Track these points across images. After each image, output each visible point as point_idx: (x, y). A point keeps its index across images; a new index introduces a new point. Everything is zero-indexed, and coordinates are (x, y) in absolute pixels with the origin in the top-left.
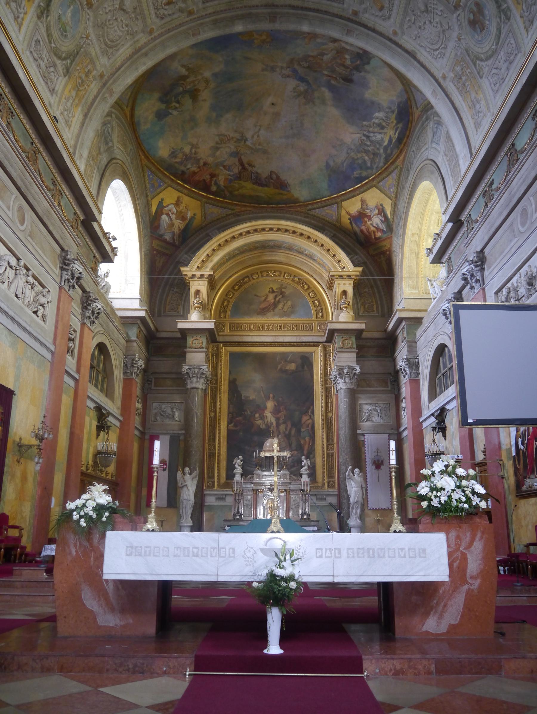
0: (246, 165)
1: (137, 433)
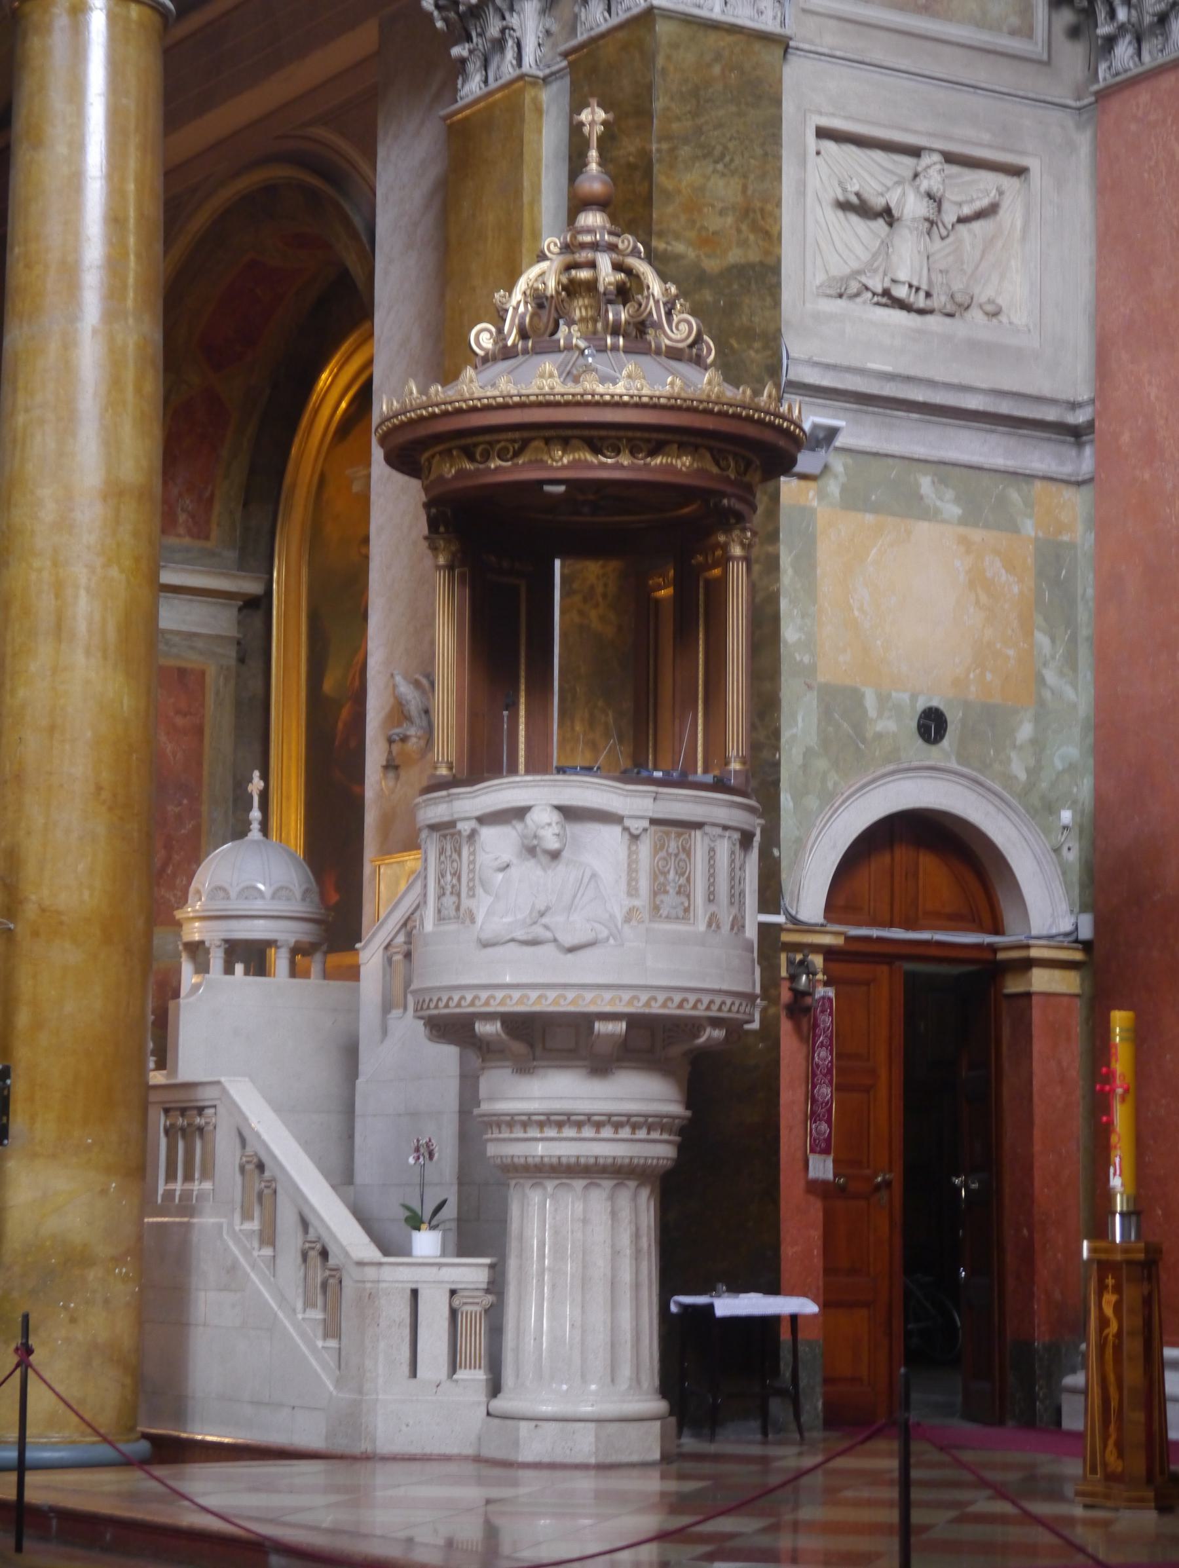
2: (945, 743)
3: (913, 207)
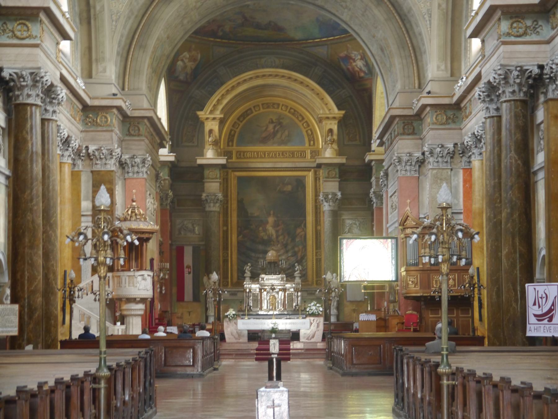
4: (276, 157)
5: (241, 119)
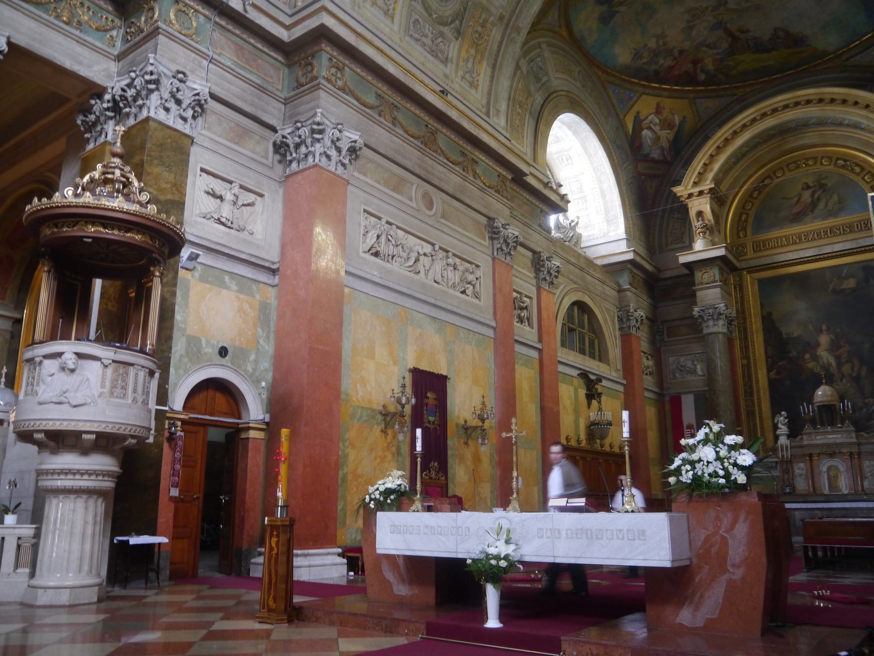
0: (737, 34)
1: (651, 395)
2: (227, 358)
3: (229, 197)
4: (821, 238)
5: (755, 194)
